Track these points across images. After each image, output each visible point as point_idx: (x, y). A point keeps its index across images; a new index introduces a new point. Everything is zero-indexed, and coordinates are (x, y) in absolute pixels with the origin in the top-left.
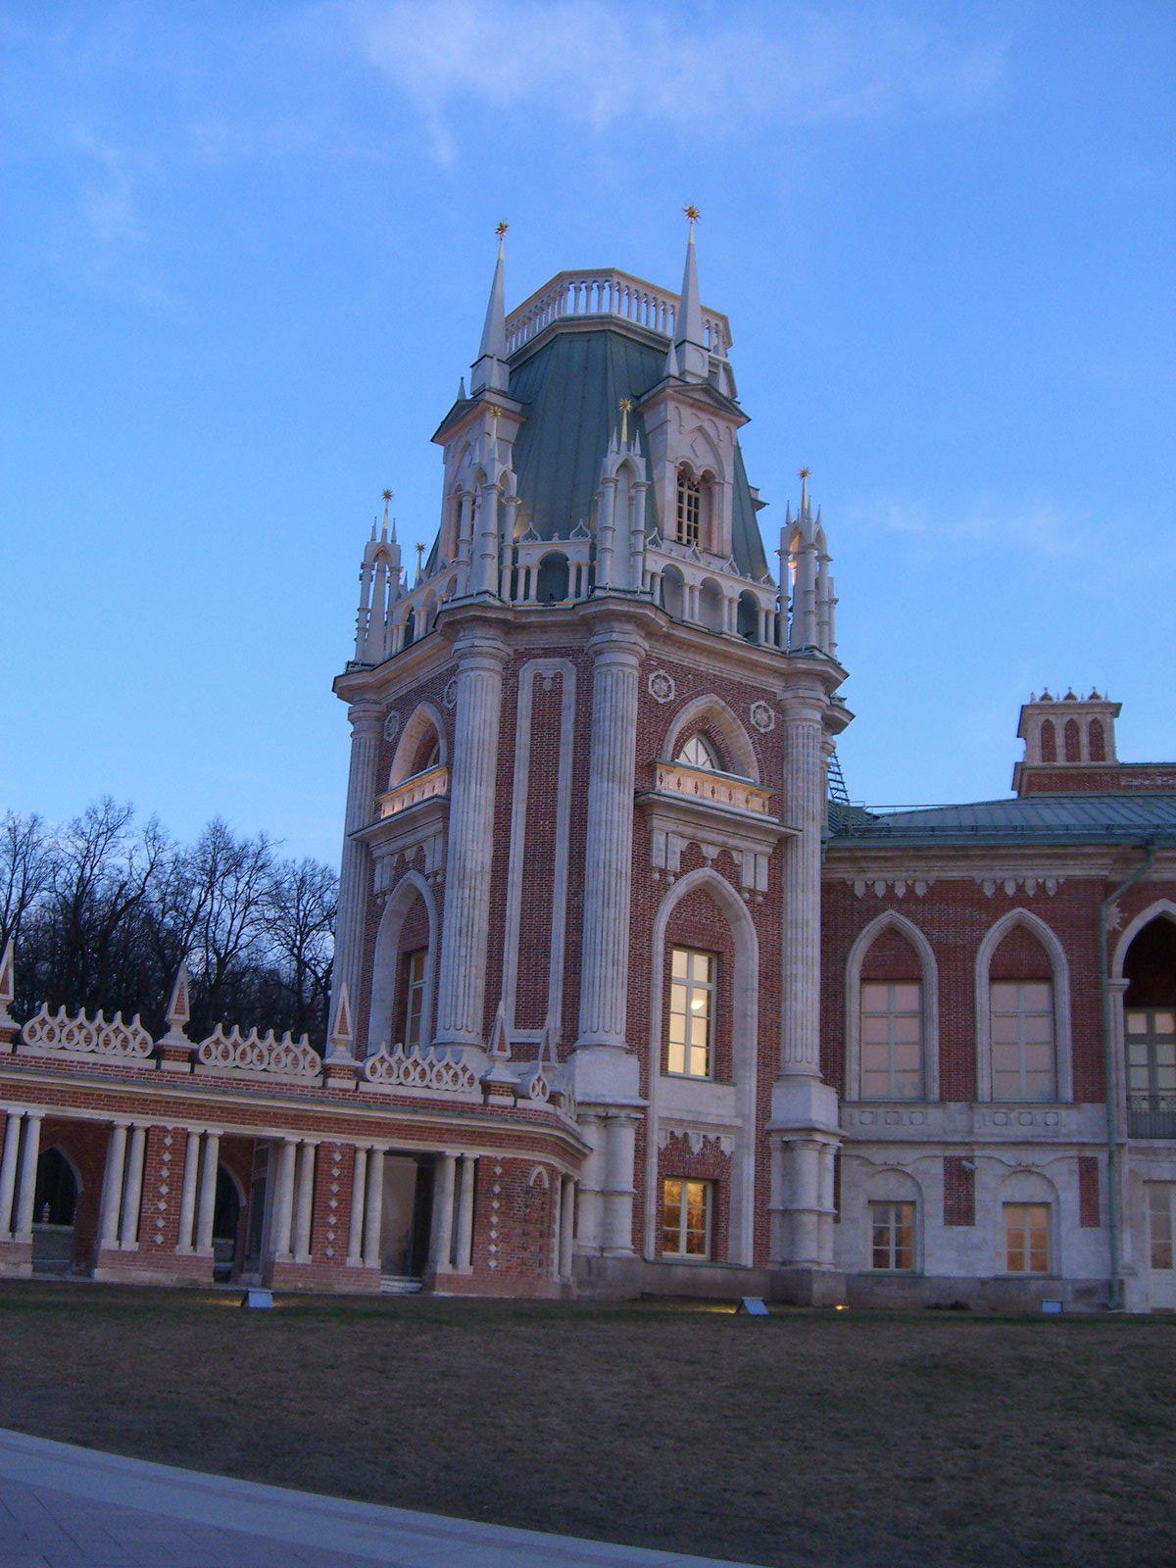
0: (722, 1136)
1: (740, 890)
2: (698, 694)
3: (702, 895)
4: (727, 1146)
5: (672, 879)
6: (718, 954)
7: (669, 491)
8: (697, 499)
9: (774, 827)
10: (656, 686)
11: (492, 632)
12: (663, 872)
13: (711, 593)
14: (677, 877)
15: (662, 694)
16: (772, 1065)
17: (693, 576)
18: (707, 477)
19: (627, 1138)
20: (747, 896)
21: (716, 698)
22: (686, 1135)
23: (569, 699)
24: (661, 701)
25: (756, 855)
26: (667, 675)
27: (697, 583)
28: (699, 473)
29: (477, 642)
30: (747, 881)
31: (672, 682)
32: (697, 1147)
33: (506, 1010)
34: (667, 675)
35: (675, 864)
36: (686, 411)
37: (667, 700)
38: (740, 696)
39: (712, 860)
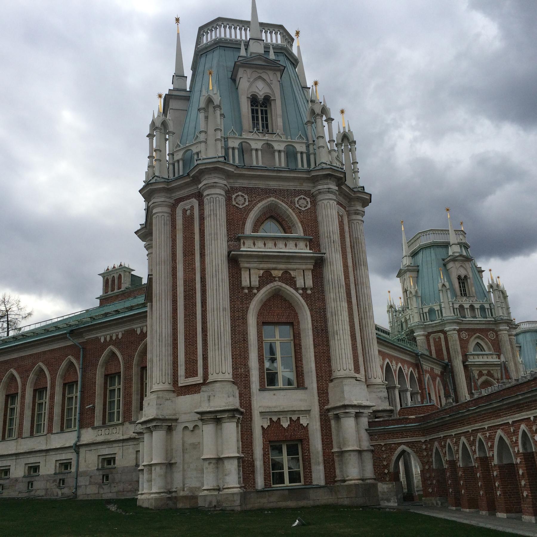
0: (301, 416)
1: (297, 289)
3: (277, 296)
4: (304, 421)
5: (255, 291)
6: (291, 324)
7: (246, 108)
8: (266, 111)
9: (312, 255)
12: (250, 288)
14: (259, 289)
16: (326, 375)
19: (231, 429)
20: (301, 291)
21: (272, 199)
22: (279, 419)
24: (241, 207)
25: (304, 271)
30: (300, 283)
32: (285, 424)
33: (181, 371)
35: (255, 282)
36: (249, 71)
38: (288, 195)
39: (279, 277)
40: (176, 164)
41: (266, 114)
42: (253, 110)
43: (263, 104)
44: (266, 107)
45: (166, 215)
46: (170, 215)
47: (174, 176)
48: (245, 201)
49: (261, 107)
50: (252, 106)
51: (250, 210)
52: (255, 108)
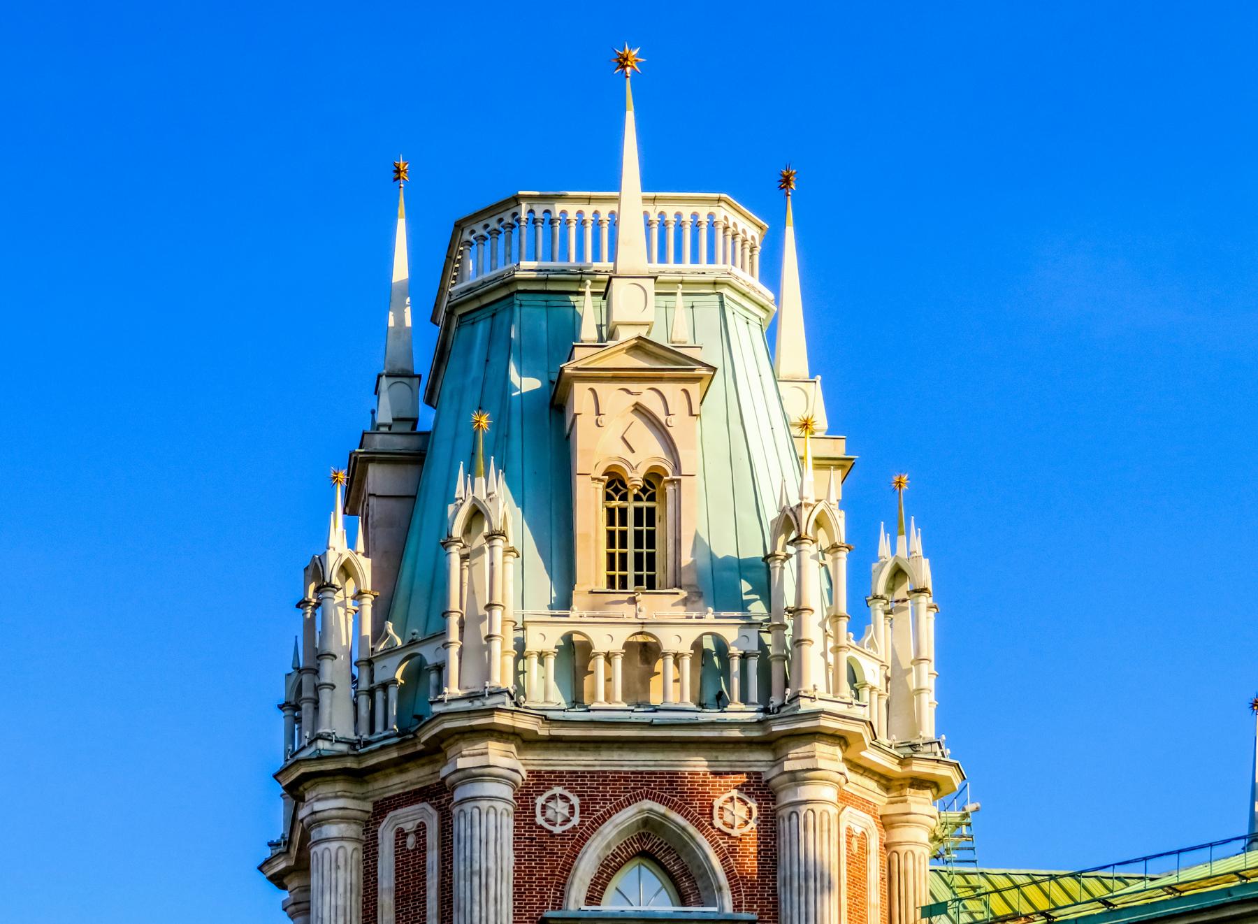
2: (620, 807)
8: (651, 511)
10: (549, 813)
11: (339, 787)
13: (645, 653)
15: (559, 820)
17: (608, 639)
18: (654, 479)
21: (647, 804)
23: (433, 857)
24: (557, 830)
26: (566, 793)
27: (617, 647)
28: (636, 479)
29: (318, 806)
31: (575, 801)
34: (566, 793)
37: (569, 826)
40: (379, 695)
41: (651, 522)
42: (611, 512)
43: (644, 490)
44: (652, 498)
45: (350, 846)
46: (360, 846)
47: (372, 730)
48: (572, 813)
49: (637, 498)
50: (609, 497)
51: (584, 839)
52: (616, 503)
